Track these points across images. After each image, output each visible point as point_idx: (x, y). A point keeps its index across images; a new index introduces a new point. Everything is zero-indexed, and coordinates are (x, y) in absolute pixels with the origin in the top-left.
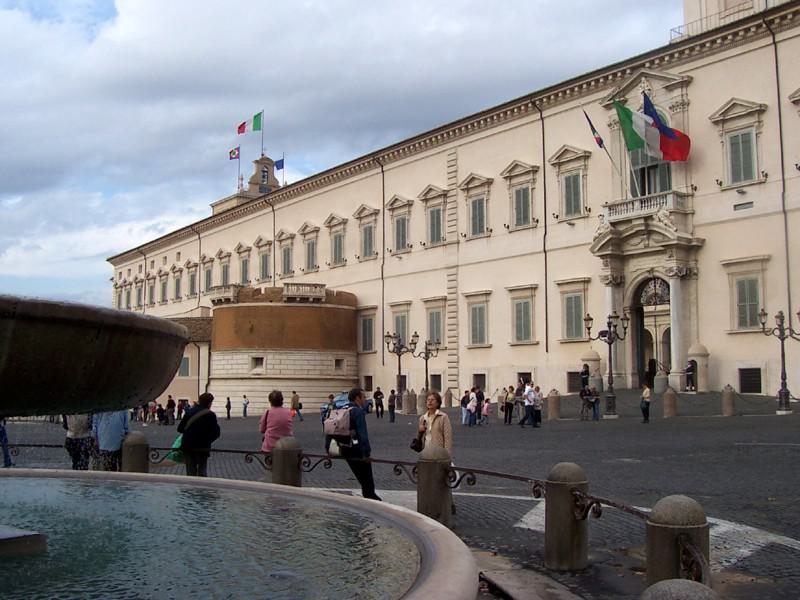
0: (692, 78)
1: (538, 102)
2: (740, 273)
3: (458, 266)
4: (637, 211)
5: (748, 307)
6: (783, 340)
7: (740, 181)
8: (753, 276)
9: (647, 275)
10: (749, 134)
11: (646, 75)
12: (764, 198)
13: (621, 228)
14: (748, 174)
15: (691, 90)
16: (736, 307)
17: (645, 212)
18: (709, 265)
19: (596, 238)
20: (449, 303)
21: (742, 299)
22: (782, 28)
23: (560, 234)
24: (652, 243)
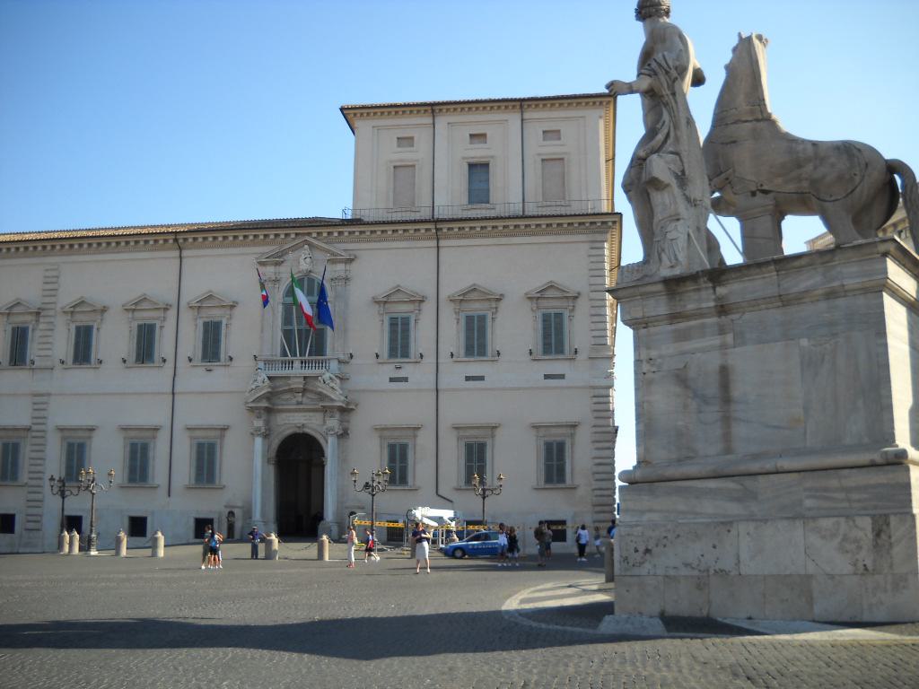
0: (356, 257)
1: (181, 241)
2: (467, 437)
3: (49, 395)
4: (297, 370)
6: (484, 498)
7: (397, 357)
8: (405, 441)
11: (311, 246)
12: (419, 375)
13: (278, 383)
14: (405, 354)
15: (354, 266)
16: (542, 467)
17: (308, 372)
18: (361, 423)
20: (34, 434)
22: (447, 237)
23: (195, 378)
24: (305, 400)
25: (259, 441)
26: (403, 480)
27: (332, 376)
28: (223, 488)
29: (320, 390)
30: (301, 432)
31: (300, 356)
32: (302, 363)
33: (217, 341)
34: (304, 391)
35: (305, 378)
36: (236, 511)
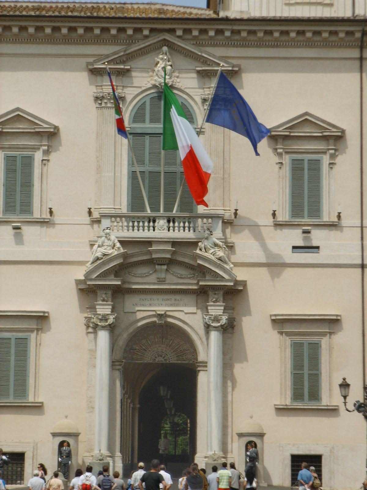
5: (306, 377)
7: (303, 217)
8: (315, 339)
9: (155, 319)
10: (318, 161)
11: (172, 47)
19: (98, 259)
21: (297, 365)
24: (170, 278)
25: (103, 336)
26: (315, 395)
27: (218, 242)
28: (38, 408)
29: (200, 262)
30: (163, 322)
31: (165, 211)
32: (169, 221)
33: (28, 185)
34: (171, 262)
35: (175, 243)
36: (71, 441)
